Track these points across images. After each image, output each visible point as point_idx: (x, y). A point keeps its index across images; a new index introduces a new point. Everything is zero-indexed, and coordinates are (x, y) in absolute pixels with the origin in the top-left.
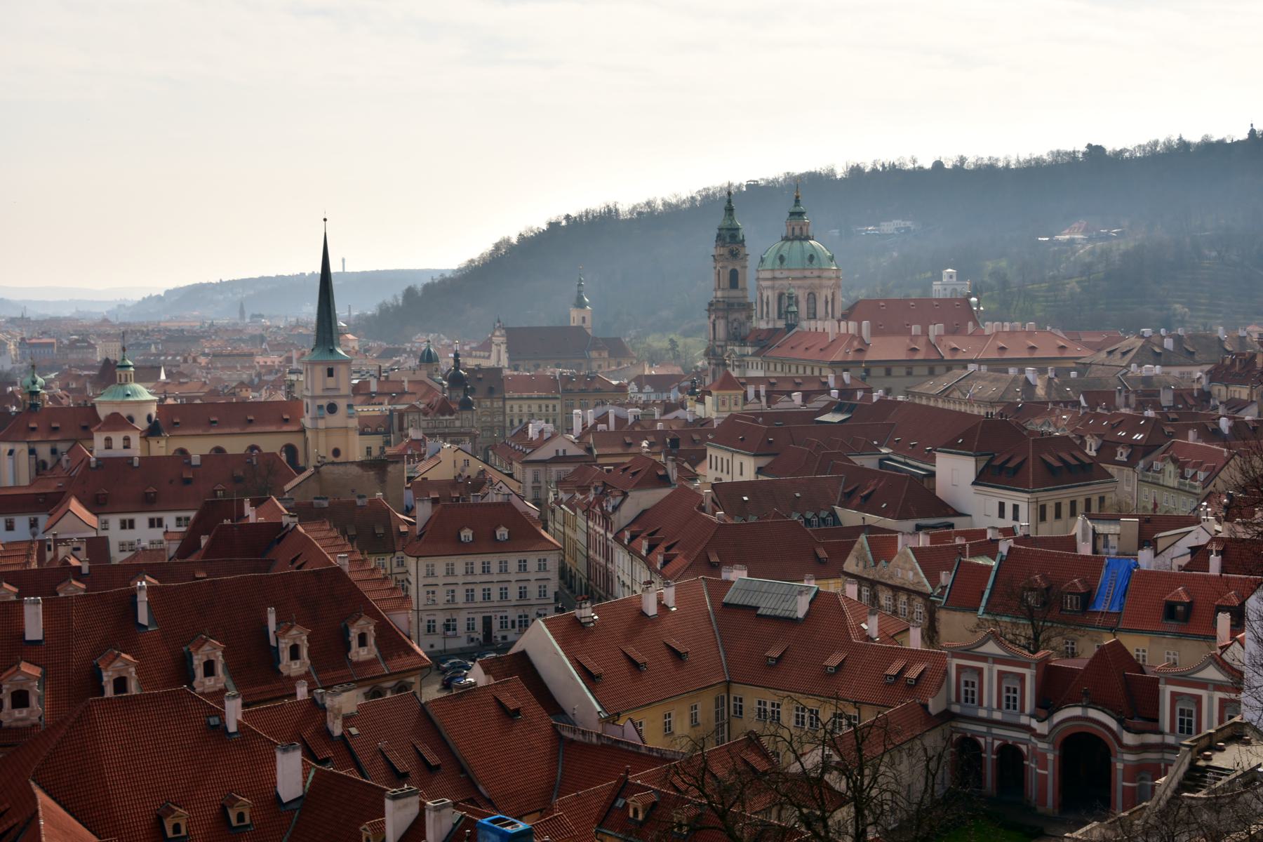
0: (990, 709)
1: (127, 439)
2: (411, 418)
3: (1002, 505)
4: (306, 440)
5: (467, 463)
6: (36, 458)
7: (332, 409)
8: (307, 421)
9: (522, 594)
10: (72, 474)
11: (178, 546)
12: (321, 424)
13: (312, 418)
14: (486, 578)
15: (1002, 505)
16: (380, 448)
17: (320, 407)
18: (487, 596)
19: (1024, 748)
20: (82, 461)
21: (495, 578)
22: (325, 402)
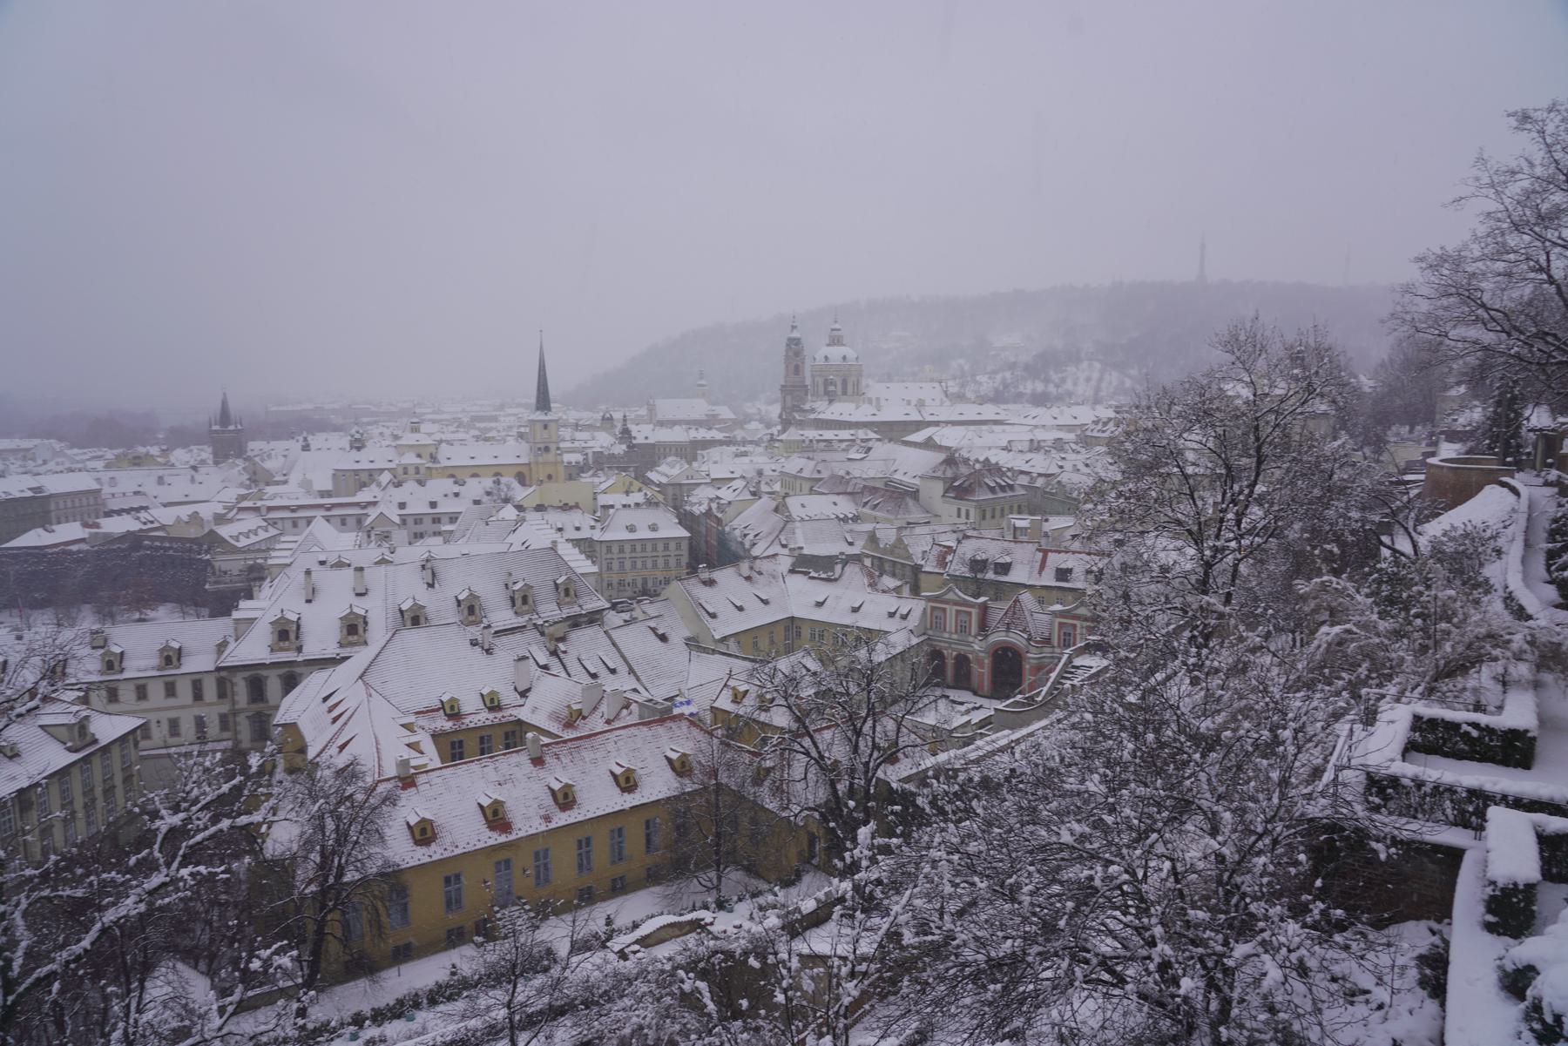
0: (951, 633)
3: (959, 509)
5: (631, 484)
7: (547, 449)
9: (667, 563)
12: (540, 459)
14: (644, 554)
15: (959, 509)
17: (539, 449)
18: (644, 565)
19: (970, 656)
21: (650, 554)
22: (542, 446)
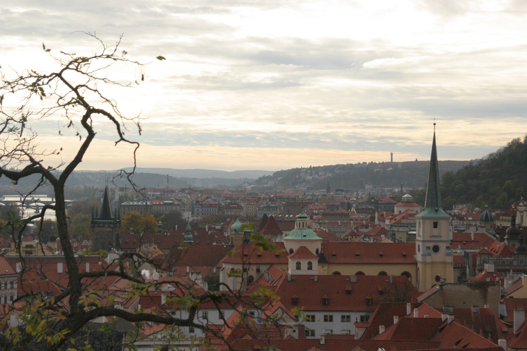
1: (310, 264)
2: (483, 258)
4: (417, 270)
6: (247, 274)
7: (436, 249)
8: (419, 257)
10: (275, 285)
11: (364, 331)
12: (428, 259)
13: (423, 255)
16: (458, 277)
17: (428, 248)
20: (281, 276)
22: (431, 245)
